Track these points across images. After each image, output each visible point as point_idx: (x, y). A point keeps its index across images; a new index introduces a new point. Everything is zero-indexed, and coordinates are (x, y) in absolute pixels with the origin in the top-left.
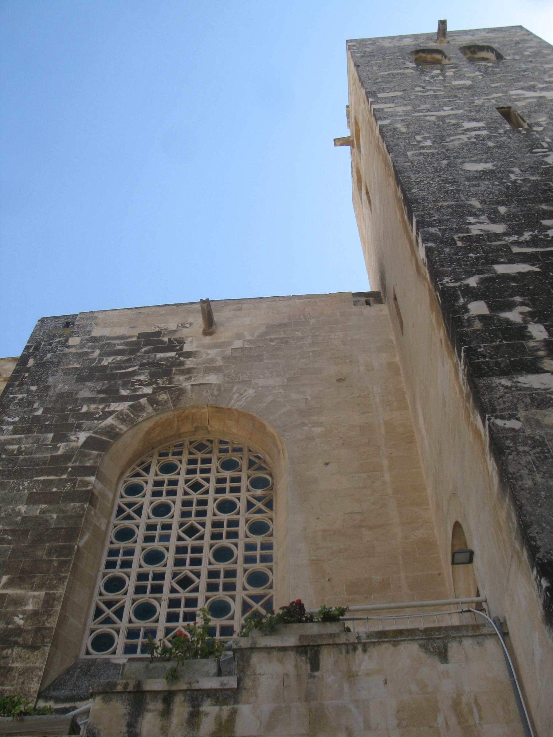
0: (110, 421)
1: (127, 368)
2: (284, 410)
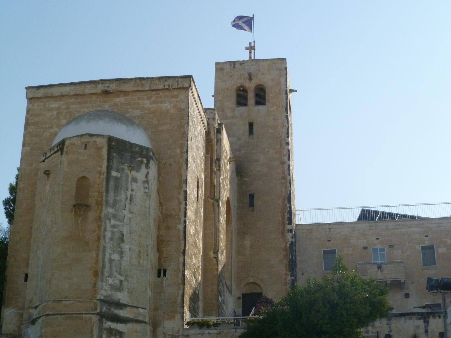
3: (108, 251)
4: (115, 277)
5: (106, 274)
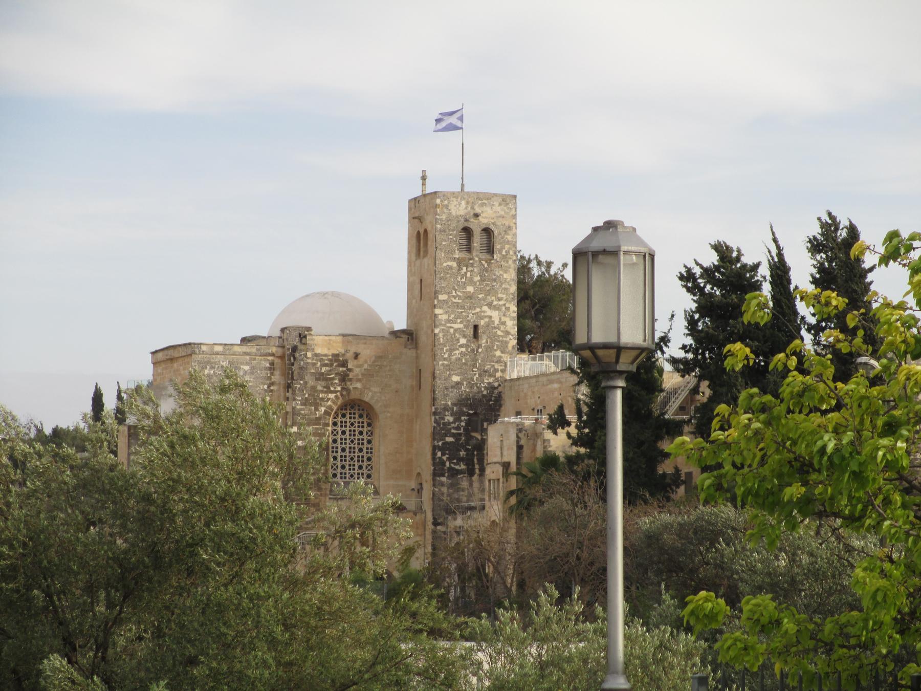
0: (329, 403)
2: (380, 404)
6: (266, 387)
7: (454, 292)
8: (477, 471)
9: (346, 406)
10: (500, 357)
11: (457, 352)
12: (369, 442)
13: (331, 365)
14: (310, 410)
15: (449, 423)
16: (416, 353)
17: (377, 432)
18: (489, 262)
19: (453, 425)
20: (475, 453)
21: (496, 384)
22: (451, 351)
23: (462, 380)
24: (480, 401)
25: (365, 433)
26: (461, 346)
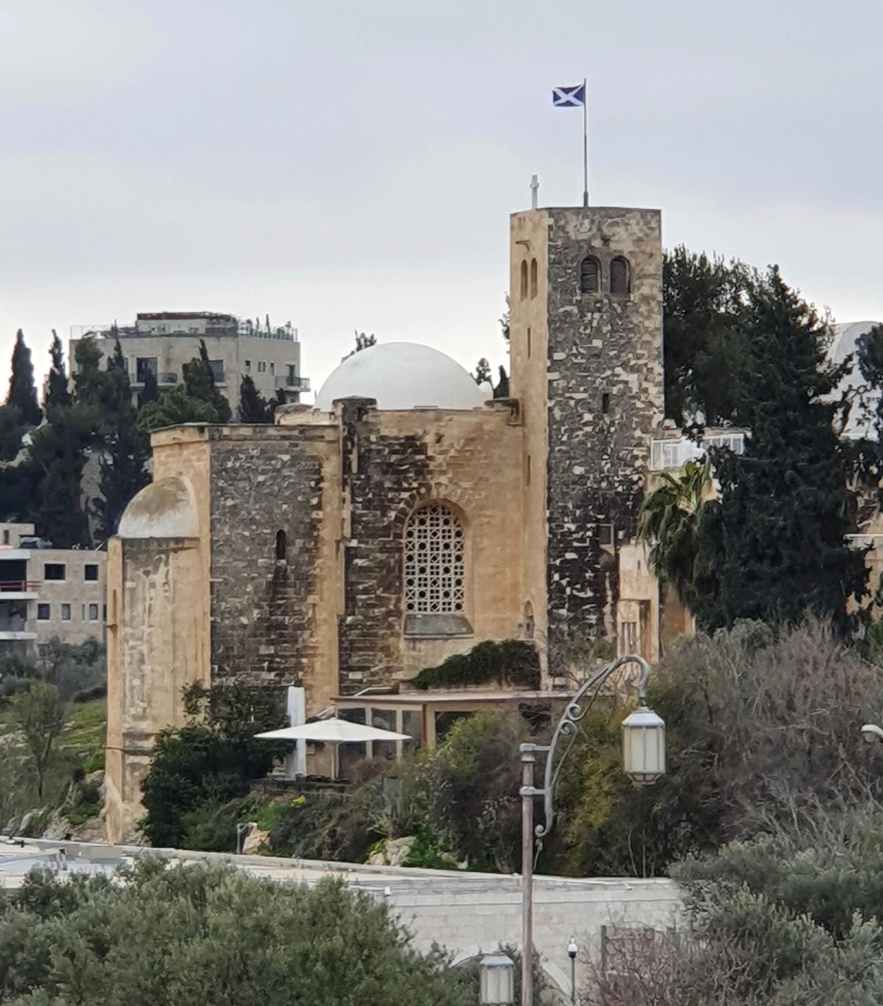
0: (402, 505)
1: (402, 466)
3: (128, 677)
4: (138, 705)
5: (128, 704)
6: (313, 484)
7: (574, 348)
8: (609, 599)
9: (425, 508)
10: (641, 438)
11: (580, 433)
12: (459, 558)
13: (404, 452)
14: (375, 515)
15: (571, 533)
16: (524, 432)
17: (468, 544)
18: (624, 307)
19: (575, 536)
20: (607, 574)
21: (635, 478)
22: (571, 431)
23: (587, 471)
24: (613, 501)
25: (452, 546)
26: (586, 424)
